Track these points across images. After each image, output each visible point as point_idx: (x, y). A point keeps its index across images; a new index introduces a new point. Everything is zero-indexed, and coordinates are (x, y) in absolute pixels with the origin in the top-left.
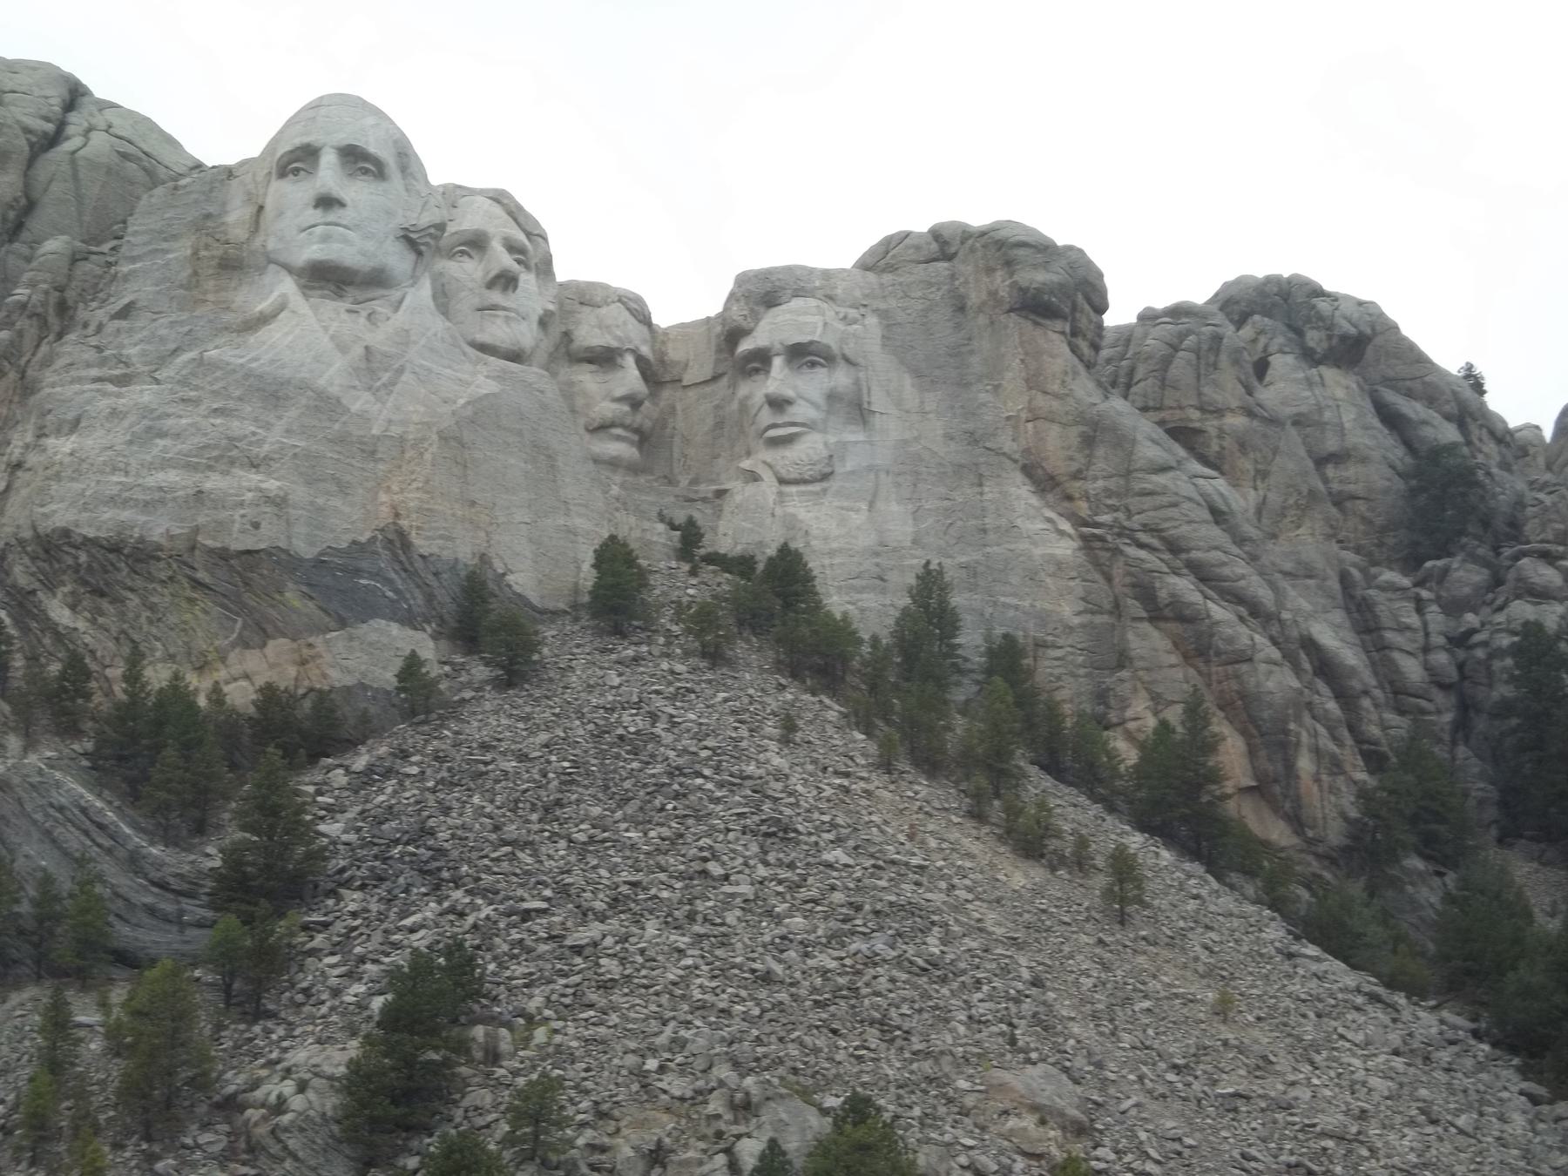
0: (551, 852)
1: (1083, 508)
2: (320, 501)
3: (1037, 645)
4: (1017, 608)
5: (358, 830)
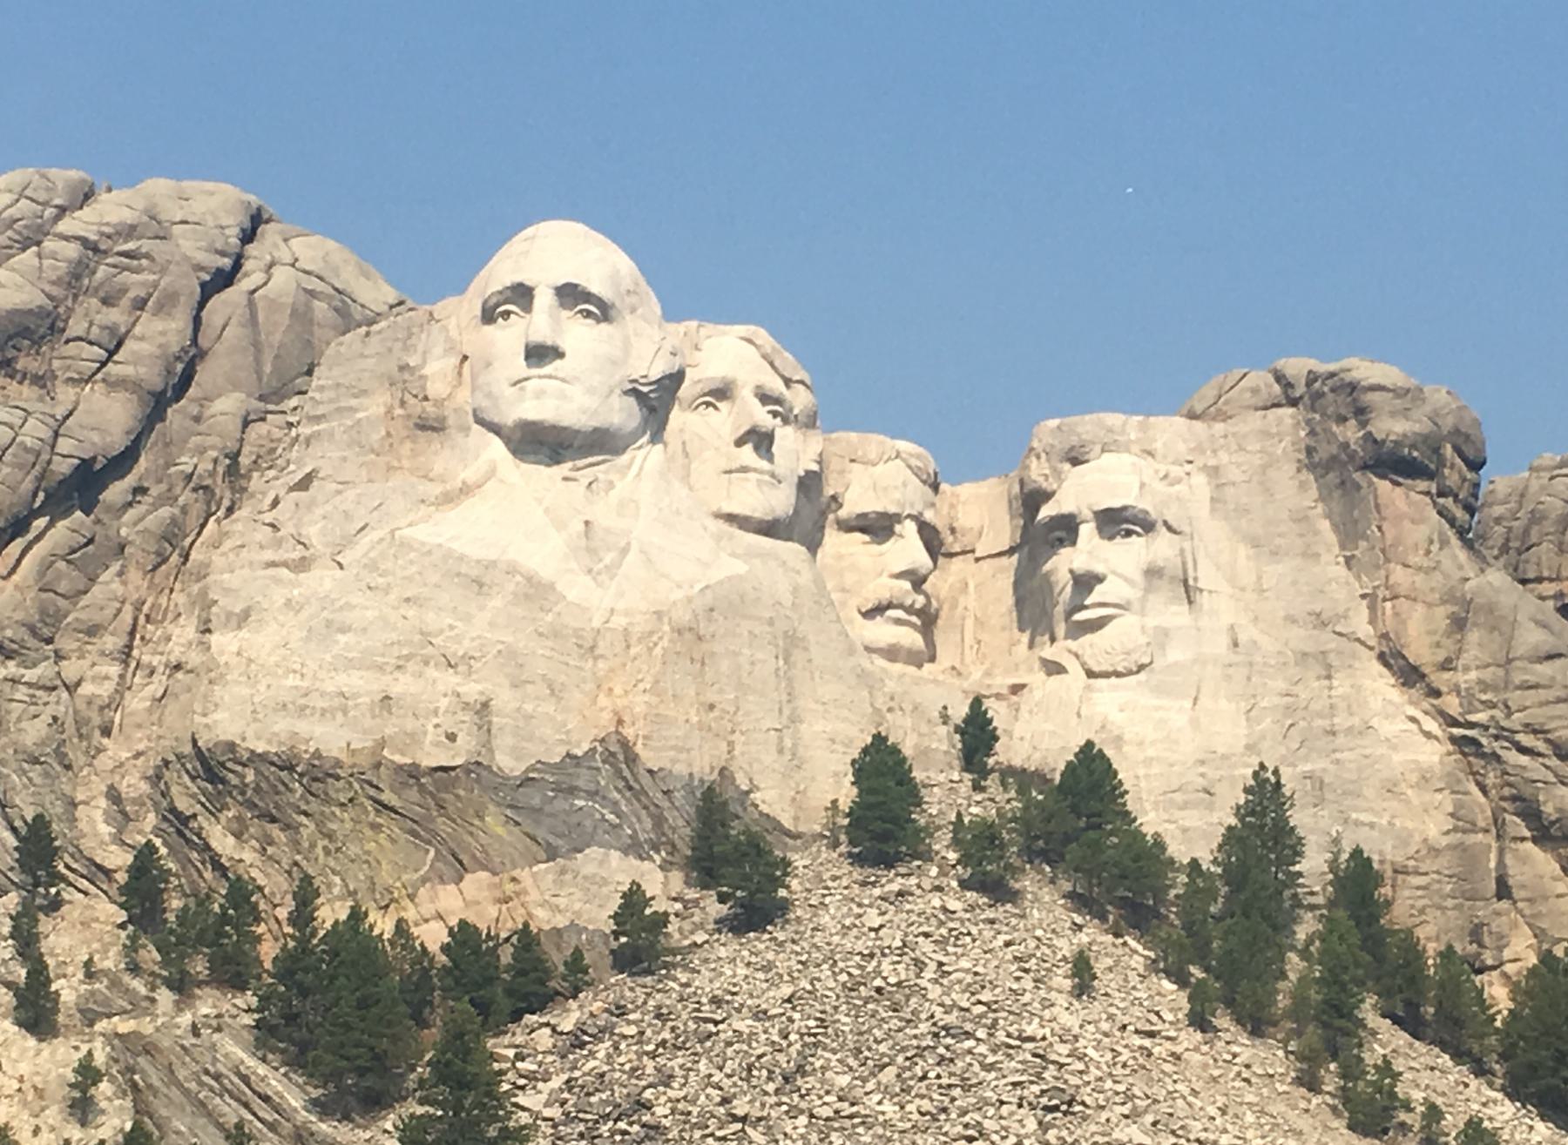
0: (788, 1130)
1: (1452, 705)
2: (529, 707)
3: (1396, 871)
4: (1372, 826)
5: (563, 1103)
